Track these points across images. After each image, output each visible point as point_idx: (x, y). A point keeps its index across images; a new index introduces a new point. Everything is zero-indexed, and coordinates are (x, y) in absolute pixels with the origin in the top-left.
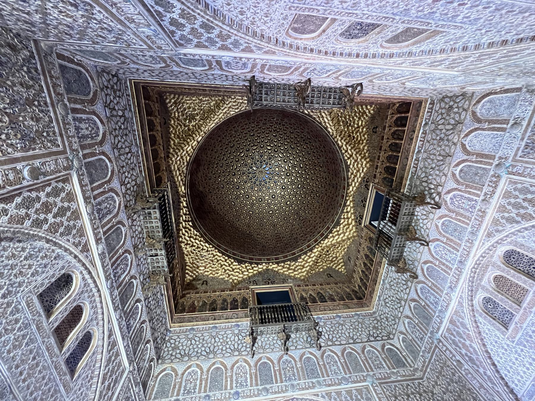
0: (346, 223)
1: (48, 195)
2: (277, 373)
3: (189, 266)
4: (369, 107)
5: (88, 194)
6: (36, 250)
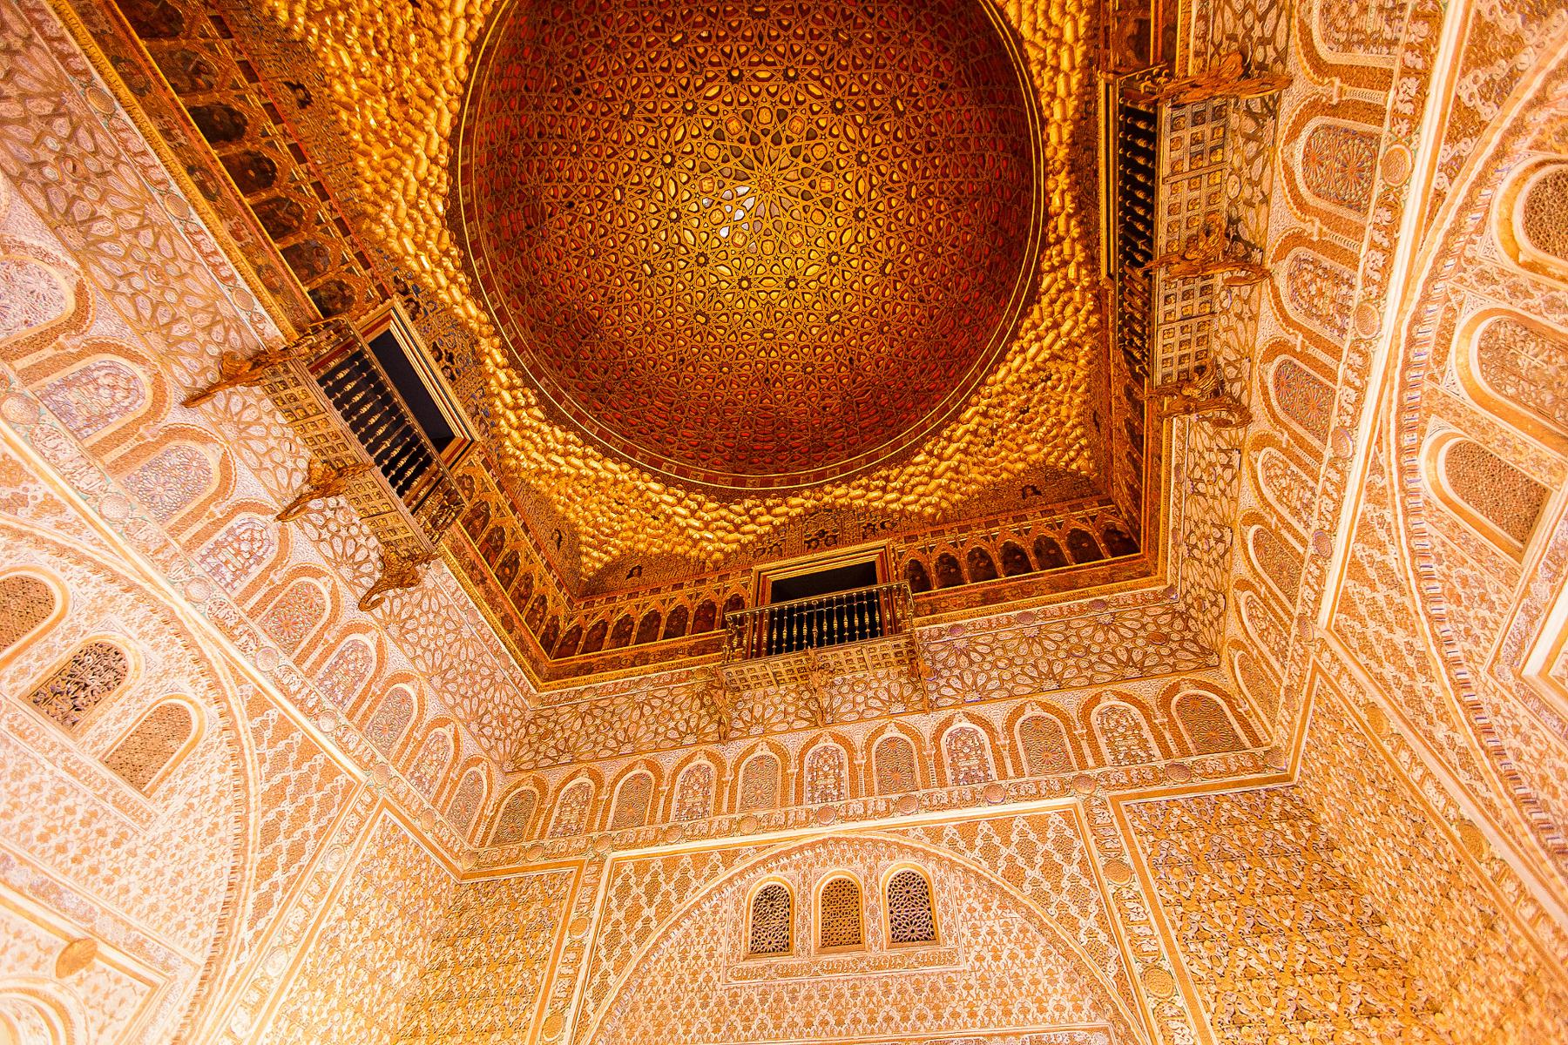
1: (619, 907)
2: (1313, 351)
3: (1049, 454)
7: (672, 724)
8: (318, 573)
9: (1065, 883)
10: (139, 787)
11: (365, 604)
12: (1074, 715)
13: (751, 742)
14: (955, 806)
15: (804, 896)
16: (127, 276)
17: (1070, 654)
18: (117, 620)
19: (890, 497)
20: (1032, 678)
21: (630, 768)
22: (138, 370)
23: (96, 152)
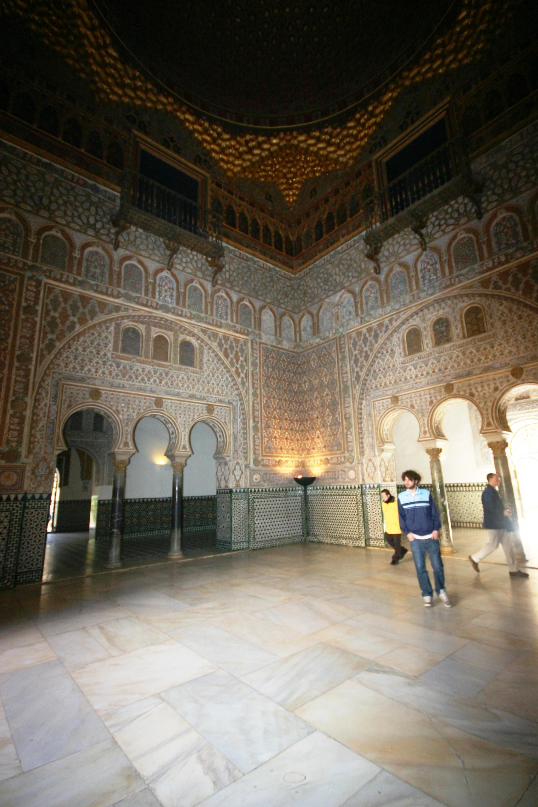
0: (128, 81)
4: (295, 198)
8: (455, 237)
10: (484, 332)
11: (479, 215)
16: (348, 277)
18: (429, 316)
22: (369, 283)
23: (323, 273)
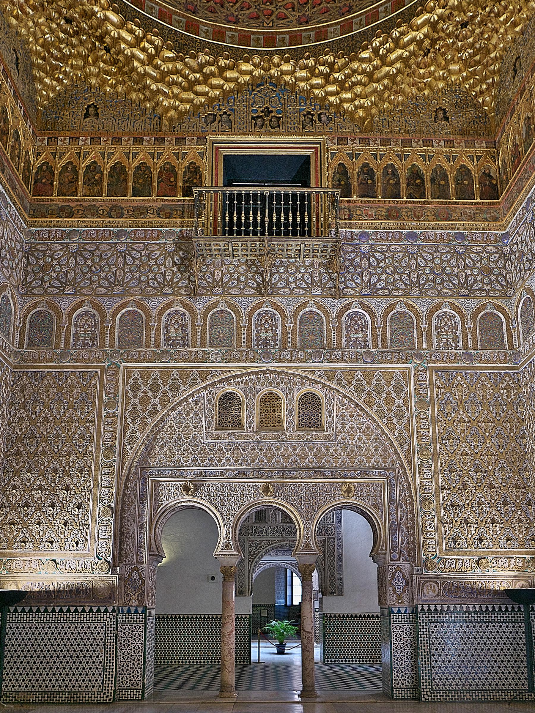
1: (135, 396)
5: (149, 355)
6: (178, 418)
7: (151, 275)
9: (394, 408)
12: (423, 314)
13: (215, 299)
14: (345, 361)
15: (250, 401)
17: (432, 272)
19: (331, 88)
20: (405, 284)
21: (124, 305)
